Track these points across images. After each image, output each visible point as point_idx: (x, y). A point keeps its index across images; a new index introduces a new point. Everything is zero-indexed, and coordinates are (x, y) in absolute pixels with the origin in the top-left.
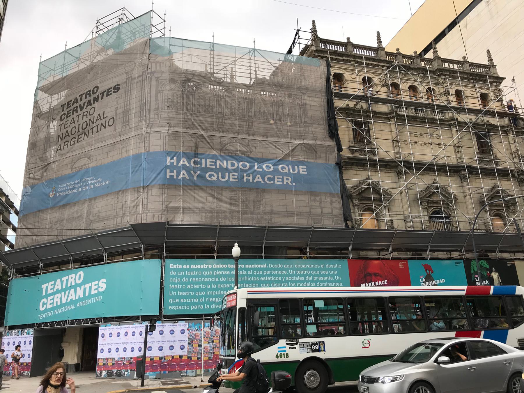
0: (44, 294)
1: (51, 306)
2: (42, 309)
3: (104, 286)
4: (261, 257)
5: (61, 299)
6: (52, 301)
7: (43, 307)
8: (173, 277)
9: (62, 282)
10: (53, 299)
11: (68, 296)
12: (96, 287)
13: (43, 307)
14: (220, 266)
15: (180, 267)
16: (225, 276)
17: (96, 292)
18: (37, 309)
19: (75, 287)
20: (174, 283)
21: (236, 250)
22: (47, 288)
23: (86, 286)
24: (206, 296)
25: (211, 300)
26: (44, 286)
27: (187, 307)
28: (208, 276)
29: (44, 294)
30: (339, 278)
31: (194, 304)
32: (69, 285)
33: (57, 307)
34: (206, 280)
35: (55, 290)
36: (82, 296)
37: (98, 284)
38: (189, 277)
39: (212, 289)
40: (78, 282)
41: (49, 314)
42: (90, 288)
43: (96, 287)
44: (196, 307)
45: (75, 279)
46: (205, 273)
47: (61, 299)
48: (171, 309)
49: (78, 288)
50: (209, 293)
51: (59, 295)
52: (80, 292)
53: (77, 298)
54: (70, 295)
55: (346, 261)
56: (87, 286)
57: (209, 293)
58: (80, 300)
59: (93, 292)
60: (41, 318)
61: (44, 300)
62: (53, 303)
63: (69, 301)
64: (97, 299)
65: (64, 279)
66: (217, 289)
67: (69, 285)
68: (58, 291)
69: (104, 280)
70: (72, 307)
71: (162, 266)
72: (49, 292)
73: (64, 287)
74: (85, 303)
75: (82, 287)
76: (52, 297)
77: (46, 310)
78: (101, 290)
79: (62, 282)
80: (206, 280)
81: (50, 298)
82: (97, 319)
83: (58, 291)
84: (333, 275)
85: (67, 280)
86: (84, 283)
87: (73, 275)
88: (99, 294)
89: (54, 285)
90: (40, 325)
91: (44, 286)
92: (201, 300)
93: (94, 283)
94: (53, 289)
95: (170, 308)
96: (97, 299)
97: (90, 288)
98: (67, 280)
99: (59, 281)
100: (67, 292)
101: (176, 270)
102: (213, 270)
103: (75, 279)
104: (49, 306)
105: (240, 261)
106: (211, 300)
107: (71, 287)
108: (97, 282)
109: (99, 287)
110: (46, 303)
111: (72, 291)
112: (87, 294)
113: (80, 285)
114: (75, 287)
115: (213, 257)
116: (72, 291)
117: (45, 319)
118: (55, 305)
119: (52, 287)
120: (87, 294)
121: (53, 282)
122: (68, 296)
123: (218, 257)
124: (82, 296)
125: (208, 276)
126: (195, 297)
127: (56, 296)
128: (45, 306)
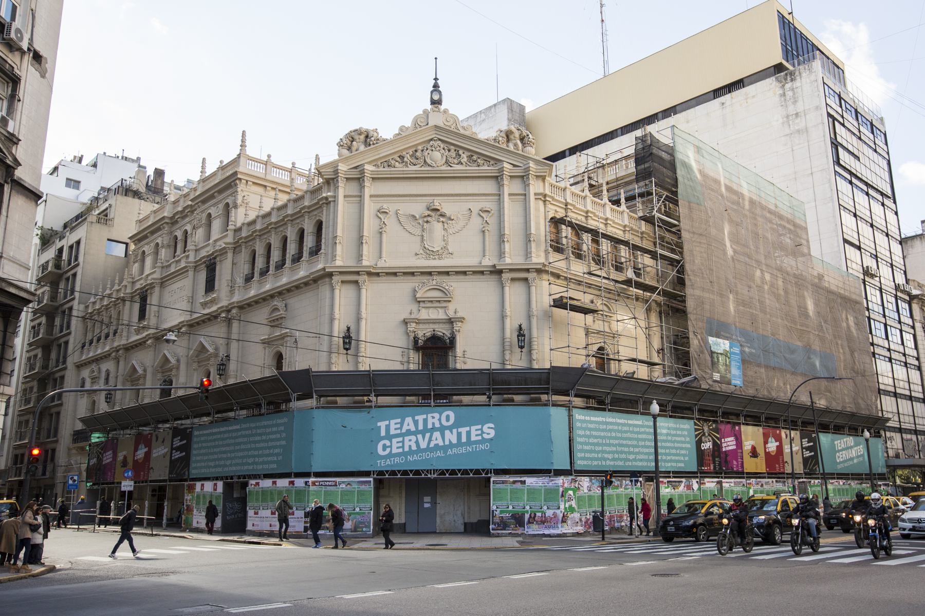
0: (383, 433)
1: (401, 450)
2: (380, 452)
3: (492, 433)
4: (637, 413)
5: (417, 442)
6: (401, 445)
7: (384, 450)
8: (581, 428)
9: (416, 423)
10: (403, 442)
11: (430, 440)
12: (479, 432)
13: (384, 450)
14: (611, 420)
15: (583, 418)
16: (615, 431)
17: (480, 438)
18: (374, 453)
19: (442, 429)
20: (581, 436)
21: (655, 408)
22: (388, 427)
23: (460, 430)
24: (603, 452)
25: (606, 456)
26: (382, 425)
27: (590, 462)
28: (603, 430)
29: (383, 433)
30: (688, 439)
31: (597, 459)
32: (430, 426)
33: (411, 452)
34: (602, 434)
35: (404, 431)
36: (454, 441)
37: (481, 429)
38: (590, 430)
39: (606, 445)
40: (445, 423)
41: (397, 460)
42: (469, 433)
43: (479, 432)
44: (595, 463)
45: (440, 420)
46: (601, 427)
47: (417, 442)
48: (580, 464)
49: (447, 432)
50: (605, 448)
51: (413, 438)
52: (451, 437)
53: (447, 443)
54: (434, 438)
55: (692, 422)
56: (464, 430)
57: (605, 448)
58: (451, 445)
59: (473, 438)
60: (382, 465)
61: (387, 443)
62: (403, 447)
63: (432, 445)
64: (482, 447)
65: (420, 418)
66: (609, 445)
67: (430, 426)
68: (409, 433)
69: (492, 426)
70: (439, 454)
71: (570, 416)
72: (393, 432)
73: (421, 427)
74: (463, 450)
75: (455, 431)
76: (401, 439)
77: (390, 455)
78: (485, 436)
79: (416, 423)
80: (602, 434)
81: (394, 441)
82: (483, 470)
83: (409, 433)
84: (684, 436)
85: (425, 421)
86: (457, 424)
87: (437, 415)
88: (483, 441)
89: (402, 423)
90: (381, 473)
91: (382, 425)
92: (600, 455)
93: (473, 428)
94: (401, 428)
95: (579, 462)
96: (482, 447)
97: (469, 433)
98: (425, 421)
99: (409, 420)
100: (428, 435)
101: (581, 421)
102: (607, 423)
103: (440, 420)
104: (395, 451)
105: (658, 419)
106: (606, 456)
107: (434, 429)
108: (479, 427)
109: (483, 432)
110: (391, 447)
111: (437, 434)
112: (464, 439)
113: (450, 428)
114: (442, 429)
115: (604, 410)
116: (437, 434)
117: (392, 466)
118: (406, 449)
119: (398, 426)
120: (464, 439)
121: (399, 420)
122: (430, 440)
123: (609, 410)
124: (454, 441)
125: (603, 430)
126: (595, 452)
127: (407, 438)
128: (388, 450)
